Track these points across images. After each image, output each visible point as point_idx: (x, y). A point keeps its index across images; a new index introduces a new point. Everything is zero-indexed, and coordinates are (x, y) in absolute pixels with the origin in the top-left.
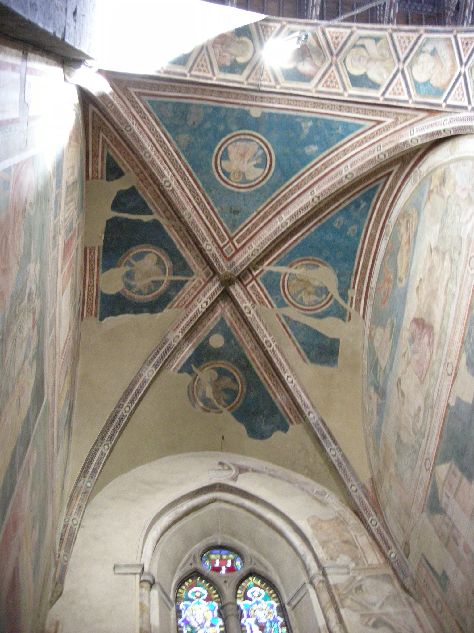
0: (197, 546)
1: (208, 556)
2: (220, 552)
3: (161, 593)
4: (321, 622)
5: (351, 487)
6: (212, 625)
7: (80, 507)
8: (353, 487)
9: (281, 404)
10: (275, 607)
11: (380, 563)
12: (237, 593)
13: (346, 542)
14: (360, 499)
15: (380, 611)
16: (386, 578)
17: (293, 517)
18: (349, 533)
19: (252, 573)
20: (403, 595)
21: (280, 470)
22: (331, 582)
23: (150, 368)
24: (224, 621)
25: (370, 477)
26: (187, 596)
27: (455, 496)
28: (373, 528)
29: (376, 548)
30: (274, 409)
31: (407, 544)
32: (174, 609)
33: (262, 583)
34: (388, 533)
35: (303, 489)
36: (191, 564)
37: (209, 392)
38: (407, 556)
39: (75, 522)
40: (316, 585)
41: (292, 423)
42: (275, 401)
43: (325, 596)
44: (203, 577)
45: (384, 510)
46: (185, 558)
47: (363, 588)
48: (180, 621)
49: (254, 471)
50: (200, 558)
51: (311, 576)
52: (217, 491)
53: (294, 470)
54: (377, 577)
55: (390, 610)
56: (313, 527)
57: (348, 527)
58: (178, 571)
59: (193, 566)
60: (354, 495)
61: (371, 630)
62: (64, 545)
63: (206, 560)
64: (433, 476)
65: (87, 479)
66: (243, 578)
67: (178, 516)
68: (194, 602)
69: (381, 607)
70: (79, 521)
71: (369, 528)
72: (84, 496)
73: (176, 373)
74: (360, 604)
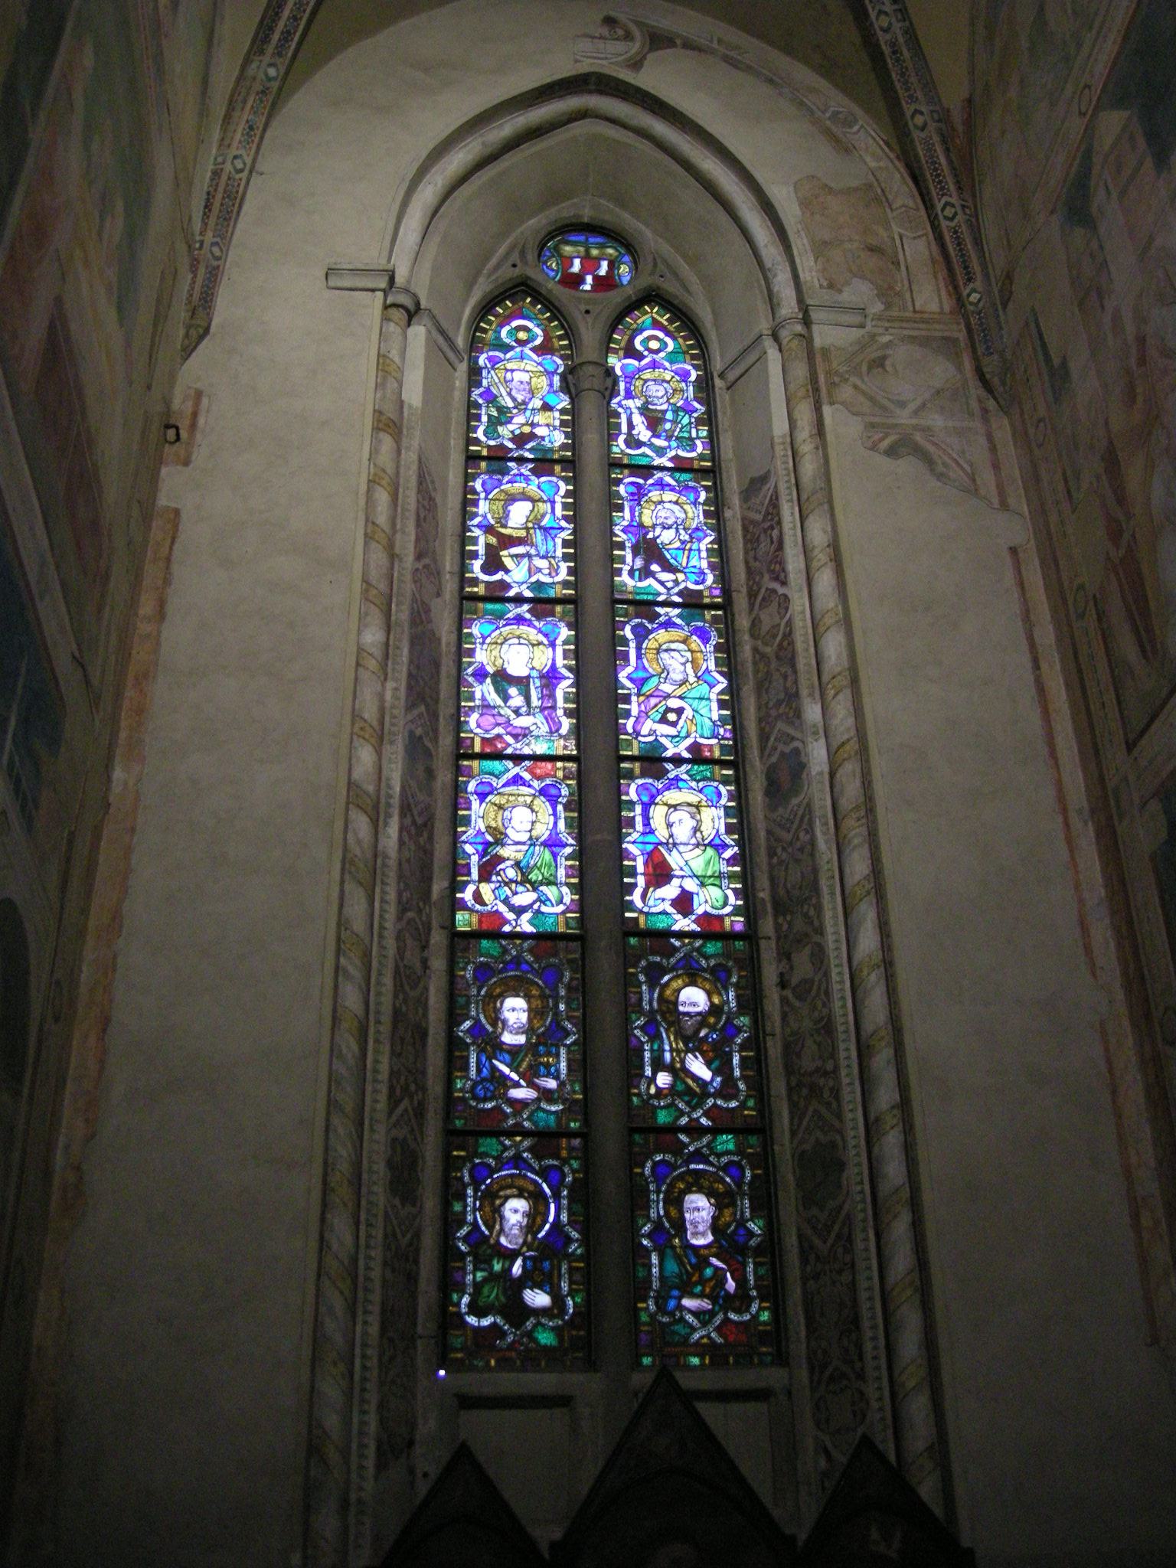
0: (531, 222)
1: (556, 248)
2: (587, 239)
3: (435, 333)
4: (780, 426)
5: (913, 117)
6: (547, 407)
7: (251, 128)
8: (919, 117)
11: (942, 312)
12: (610, 339)
13: (872, 249)
14: (930, 149)
15: (914, 421)
16: (947, 346)
17: (759, 176)
18: (887, 227)
20: (975, 390)
21: (752, 47)
22: (818, 342)
24: (572, 401)
25: (966, 95)
26: (498, 338)
27: (1123, 193)
28: (944, 224)
29: (942, 274)
31: (1009, 277)
32: (463, 367)
34: (978, 242)
35: (802, 104)
36: (514, 266)
38: (1005, 305)
39: (240, 166)
40: (784, 342)
43: (800, 371)
44: (538, 297)
45: (980, 182)
46: (502, 251)
47: (888, 363)
49: (688, 45)
50: (536, 254)
51: (778, 320)
52: (590, 92)
53: (789, 50)
54: (924, 342)
55: (936, 421)
56: (805, 204)
57: (888, 210)
58: (481, 280)
59: (517, 271)
60: (916, 134)
62: (212, 222)
63: (550, 258)
64: (1089, 131)
65: (267, 59)
66: (629, 306)
67: (489, 150)
69: (916, 413)
70: (249, 161)
71: (936, 223)
74: (871, 399)
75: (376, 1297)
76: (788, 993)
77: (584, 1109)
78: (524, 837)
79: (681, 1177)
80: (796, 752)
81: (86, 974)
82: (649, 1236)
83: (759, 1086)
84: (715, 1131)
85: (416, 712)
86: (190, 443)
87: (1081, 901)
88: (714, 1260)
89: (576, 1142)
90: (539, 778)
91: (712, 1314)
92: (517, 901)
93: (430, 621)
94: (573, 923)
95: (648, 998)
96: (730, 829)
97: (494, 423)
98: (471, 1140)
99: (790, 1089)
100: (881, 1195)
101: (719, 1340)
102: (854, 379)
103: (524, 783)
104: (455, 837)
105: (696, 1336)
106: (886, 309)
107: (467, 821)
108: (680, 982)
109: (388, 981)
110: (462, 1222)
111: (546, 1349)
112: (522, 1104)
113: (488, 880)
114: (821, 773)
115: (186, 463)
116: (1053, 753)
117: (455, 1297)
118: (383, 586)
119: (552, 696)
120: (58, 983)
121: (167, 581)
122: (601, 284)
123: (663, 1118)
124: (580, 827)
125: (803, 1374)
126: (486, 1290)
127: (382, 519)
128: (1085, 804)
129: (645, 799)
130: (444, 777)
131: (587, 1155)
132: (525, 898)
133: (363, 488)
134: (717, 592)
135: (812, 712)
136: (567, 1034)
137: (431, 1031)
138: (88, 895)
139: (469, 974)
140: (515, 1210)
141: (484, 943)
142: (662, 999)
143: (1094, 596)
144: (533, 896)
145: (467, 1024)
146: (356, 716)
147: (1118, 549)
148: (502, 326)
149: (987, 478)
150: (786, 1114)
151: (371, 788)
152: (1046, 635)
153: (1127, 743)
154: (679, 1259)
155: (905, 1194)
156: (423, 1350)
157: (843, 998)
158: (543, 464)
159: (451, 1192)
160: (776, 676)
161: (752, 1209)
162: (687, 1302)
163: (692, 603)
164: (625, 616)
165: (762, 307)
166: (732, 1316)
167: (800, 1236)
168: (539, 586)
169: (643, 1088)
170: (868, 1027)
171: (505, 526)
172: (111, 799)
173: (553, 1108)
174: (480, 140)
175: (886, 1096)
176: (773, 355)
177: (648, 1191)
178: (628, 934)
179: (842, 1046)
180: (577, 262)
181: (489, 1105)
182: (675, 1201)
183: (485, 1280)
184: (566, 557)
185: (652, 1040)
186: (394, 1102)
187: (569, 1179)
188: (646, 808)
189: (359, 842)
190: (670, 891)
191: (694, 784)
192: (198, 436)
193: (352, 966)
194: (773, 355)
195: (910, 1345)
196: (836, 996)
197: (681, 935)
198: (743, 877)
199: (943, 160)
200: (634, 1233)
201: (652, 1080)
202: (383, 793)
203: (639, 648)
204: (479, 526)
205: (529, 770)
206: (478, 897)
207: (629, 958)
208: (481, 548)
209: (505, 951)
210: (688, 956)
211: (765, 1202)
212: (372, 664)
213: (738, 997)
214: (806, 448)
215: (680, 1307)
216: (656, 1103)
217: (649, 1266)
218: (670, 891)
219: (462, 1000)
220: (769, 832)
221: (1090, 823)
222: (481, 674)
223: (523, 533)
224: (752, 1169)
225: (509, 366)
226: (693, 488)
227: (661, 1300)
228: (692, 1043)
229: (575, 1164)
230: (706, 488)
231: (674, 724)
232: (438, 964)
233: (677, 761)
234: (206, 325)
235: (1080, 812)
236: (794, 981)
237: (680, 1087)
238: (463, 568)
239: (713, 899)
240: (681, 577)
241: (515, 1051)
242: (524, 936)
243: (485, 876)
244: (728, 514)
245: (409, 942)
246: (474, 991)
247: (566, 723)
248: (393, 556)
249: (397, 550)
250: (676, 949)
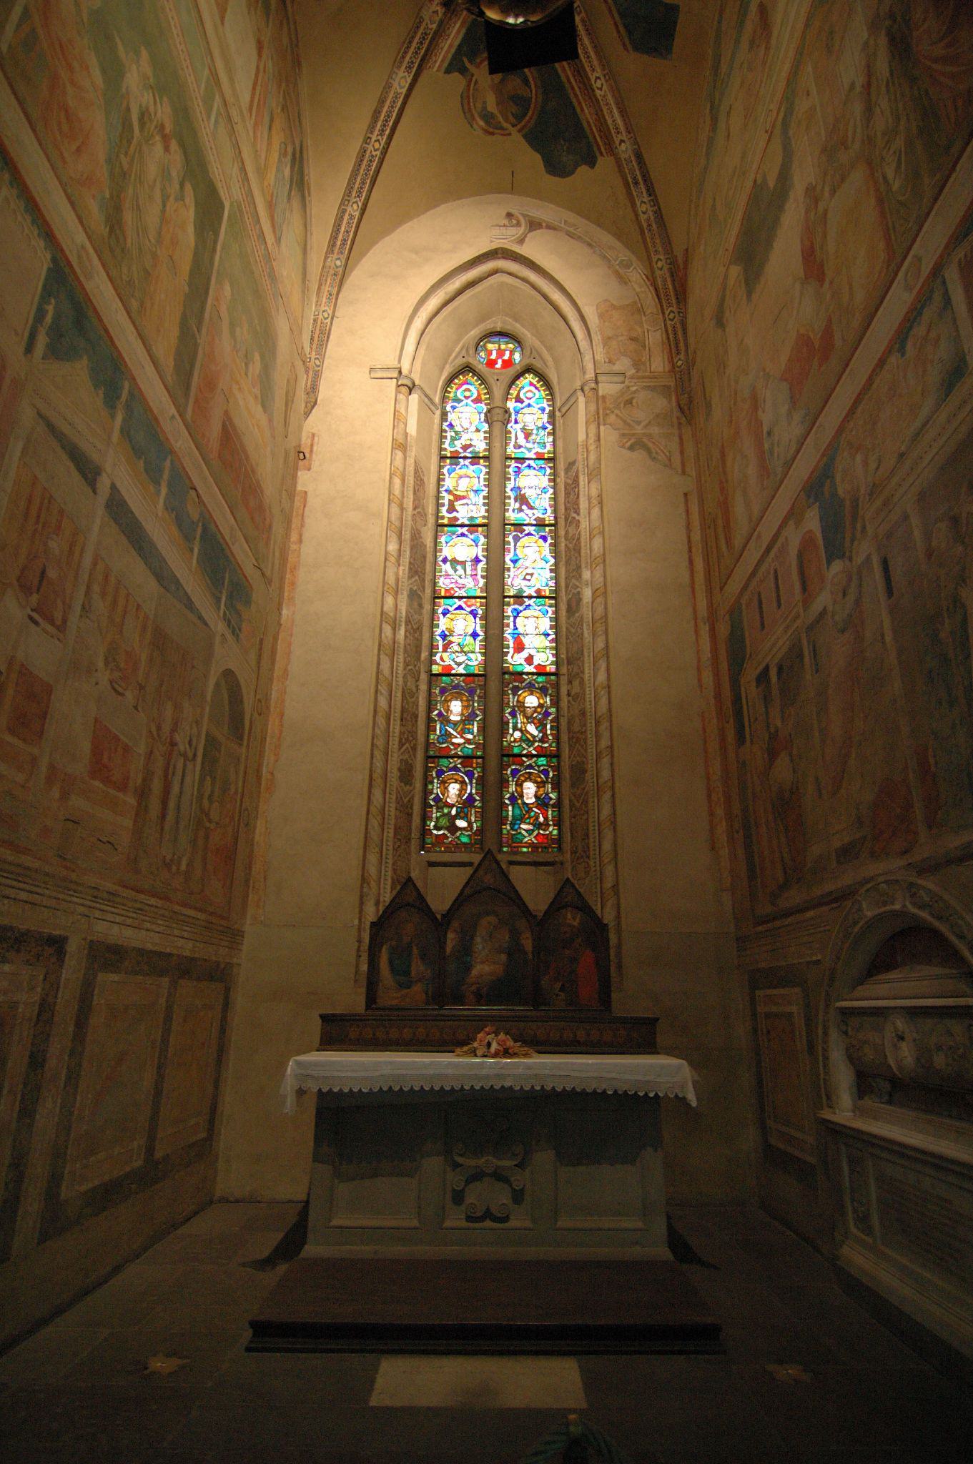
0: (472, 333)
3: (423, 397)
4: (581, 437)
6: (478, 430)
7: (331, 295)
9: (588, 122)
10: (547, 411)
12: (508, 394)
13: (632, 339)
18: (642, 326)
19: (528, 369)
20: (677, 413)
23: (401, 73)
24: (489, 428)
25: (685, 247)
28: (669, 323)
30: (578, 132)
32: (438, 413)
33: (538, 382)
35: (605, 257)
37: (491, 103)
39: (326, 316)
41: (601, 154)
42: (581, 117)
43: (593, 407)
44: (475, 373)
46: (457, 349)
47: (634, 401)
48: (446, 424)
49: (549, 227)
56: (601, 316)
58: (447, 366)
61: (625, 452)
62: (314, 347)
67: (447, 298)
68: (461, 404)
69: (646, 427)
70: (330, 312)
72: (334, 280)
73: (441, 74)
75: (393, 822)
76: (570, 698)
77: (483, 747)
78: (462, 632)
79: (522, 775)
80: (579, 593)
81: (274, 695)
82: (509, 799)
83: (557, 738)
84: (538, 756)
85: (413, 580)
86: (310, 459)
88: (535, 809)
89: (480, 761)
90: (469, 606)
91: (533, 831)
92: (458, 660)
93: (421, 537)
94: (481, 669)
95: (512, 700)
96: (551, 627)
97: (453, 439)
98: (436, 760)
99: (569, 739)
100: (600, 784)
101: (536, 842)
102: (617, 411)
103: (463, 609)
104: (432, 633)
105: (526, 840)
106: (637, 372)
107: (438, 626)
108: (526, 694)
109: (399, 695)
110: (432, 793)
111: (464, 844)
112: (459, 745)
113: (446, 652)
114: (588, 603)
115: (309, 470)
117: (428, 823)
118: (397, 523)
119: (476, 569)
120: (260, 701)
121: (302, 526)
122: (507, 364)
123: (516, 751)
124: (486, 628)
125: (568, 856)
126: (441, 820)
127: (397, 492)
128: (706, 615)
129: (515, 614)
130: (427, 607)
131: (484, 767)
132: (461, 658)
133: (388, 477)
134: (552, 518)
135: (586, 575)
136: (477, 716)
137: (420, 715)
138: (273, 663)
139: (437, 691)
140: (454, 789)
141: (444, 678)
142: (518, 701)
144: (466, 658)
145: (436, 712)
146: (384, 583)
148: (457, 389)
149: (677, 460)
150: (567, 749)
151: (392, 614)
152: (697, 536)
154: (520, 807)
155: (610, 784)
156: (414, 844)
157: (591, 701)
158: (475, 459)
159: (427, 781)
160: (573, 558)
161: (552, 788)
162: (523, 826)
163: (540, 524)
164: (510, 531)
165: (578, 374)
166: (541, 832)
167: (570, 801)
168: (472, 518)
169: (508, 738)
170: (599, 714)
171: (456, 490)
172: (282, 622)
173: (471, 747)
174: (443, 291)
175: (604, 743)
176: (581, 400)
177: (508, 781)
178: (505, 673)
179: (589, 721)
180: (494, 353)
181: (444, 746)
182: (520, 785)
183: (441, 816)
184: (484, 504)
185: (513, 719)
186: (401, 745)
187: (476, 775)
188: (515, 618)
189: (386, 637)
190: (524, 654)
191: (537, 608)
192: (314, 456)
193: (383, 689)
194: (581, 400)
195: (607, 846)
196: (588, 700)
197: (528, 674)
198: (556, 648)
199: (671, 287)
200: (502, 797)
201: (512, 735)
202: (398, 616)
203: (515, 546)
204: (446, 491)
205: (465, 603)
206: (442, 659)
207: (504, 684)
208: (446, 502)
209: (453, 681)
210: (530, 683)
211: (557, 786)
212: (393, 560)
213: (551, 700)
214: (592, 448)
215: (520, 828)
216: (513, 744)
217: (508, 811)
218: (524, 654)
219: (434, 703)
220: (567, 628)
222: (445, 561)
223: (465, 494)
224: (553, 771)
225: (460, 410)
226: (545, 468)
227: (512, 825)
228: (530, 719)
229: (479, 770)
230: (550, 467)
231: (529, 580)
232: (423, 687)
233: (530, 597)
234: (314, 400)
236: (573, 693)
237: (524, 738)
238: (438, 511)
239: (540, 659)
240: (535, 511)
241: (455, 724)
242: (461, 675)
243: (445, 650)
244: (558, 480)
245: (409, 677)
246: (439, 698)
247: (482, 582)
248: (402, 509)
249: (405, 506)
250: (525, 680)
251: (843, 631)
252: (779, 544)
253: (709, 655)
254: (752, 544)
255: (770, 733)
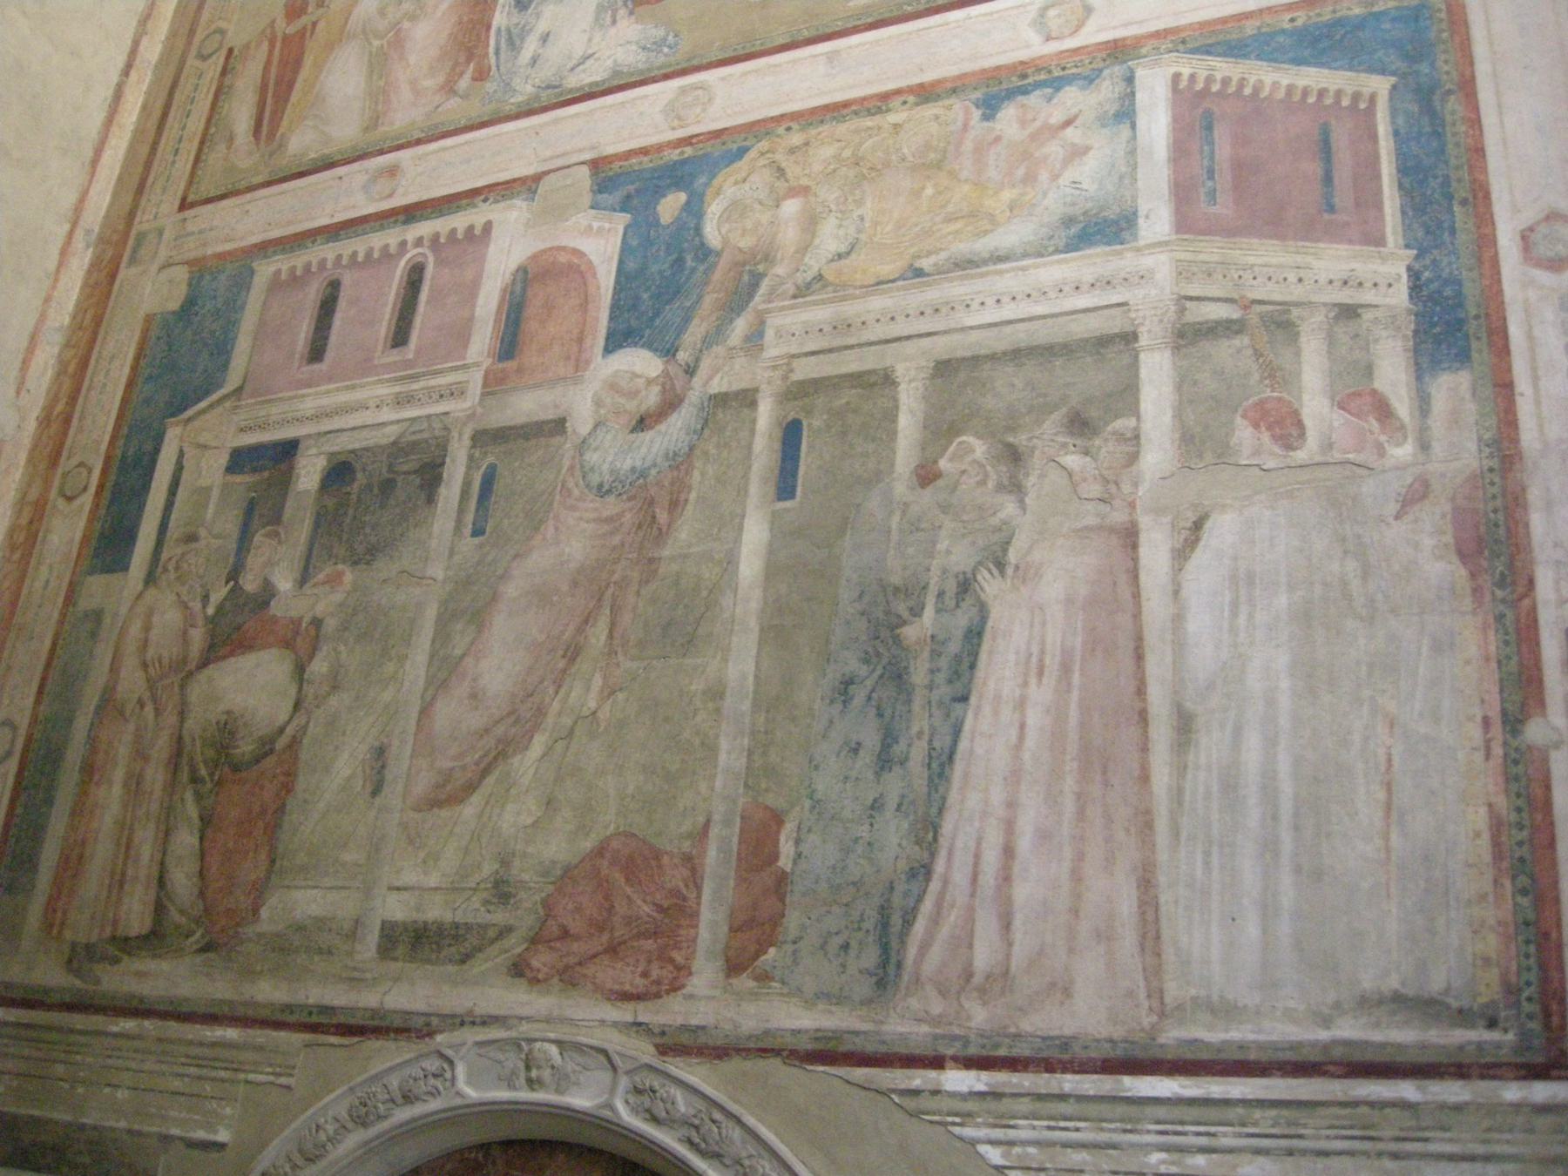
87: (42, 317)
116: (95, 162)
128: (97, 228)
143: (231, 51)
147: (288, 25)
152: (152, 51)
153: (184, 199)
221: (91, 249)
235: (88, 232)
251: (602, 491)
252: (458, 221)
253: (67, 321)
254: (356, 173)
255: (236, 590)
